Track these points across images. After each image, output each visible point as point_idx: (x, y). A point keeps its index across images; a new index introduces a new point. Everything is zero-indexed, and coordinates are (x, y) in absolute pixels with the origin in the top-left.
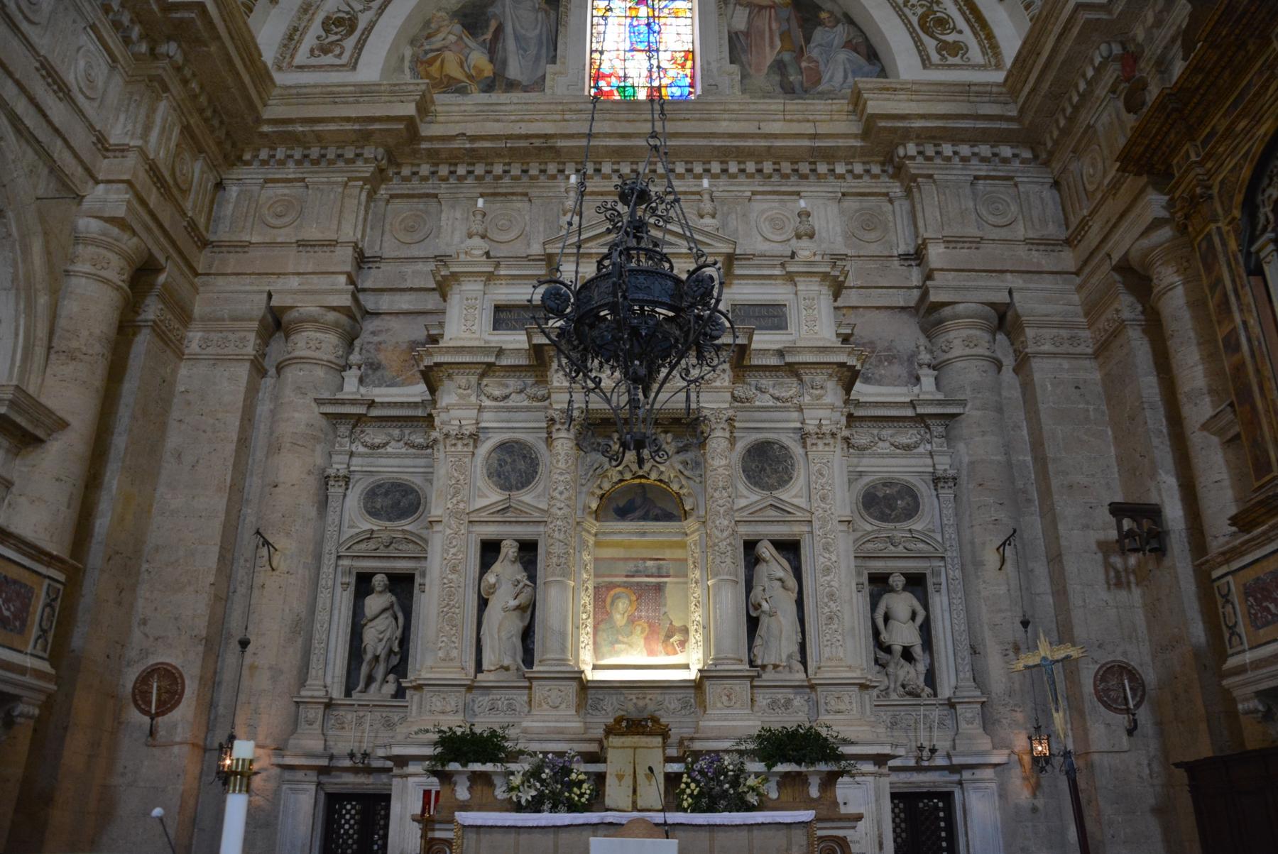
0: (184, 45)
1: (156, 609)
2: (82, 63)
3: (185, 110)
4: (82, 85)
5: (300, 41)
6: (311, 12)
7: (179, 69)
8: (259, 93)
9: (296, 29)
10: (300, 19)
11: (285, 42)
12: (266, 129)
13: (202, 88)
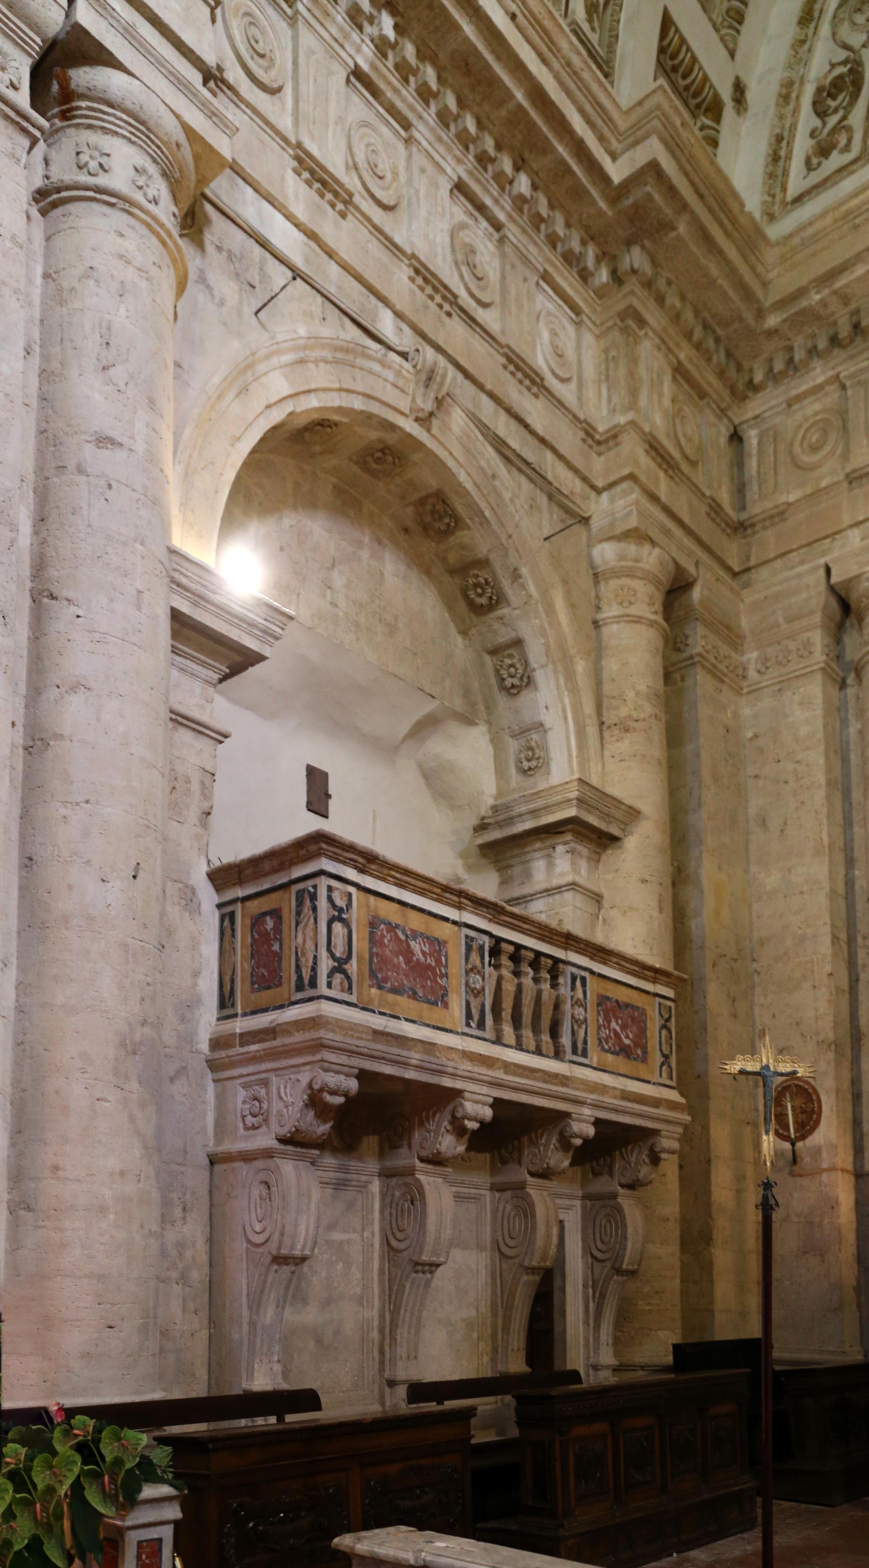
0: (647, 243)
1: (774, 1016)
2: (545, 335)
3: (671, 344)
4: (553, 365)
5: (788, 157)
6: (794, 95)
7: (648, 284)
8: (753, 269)
9: (779, 139)
10: (781, 117)
11: (771, 168)
12: (773, 321)
13: (683, 298)
